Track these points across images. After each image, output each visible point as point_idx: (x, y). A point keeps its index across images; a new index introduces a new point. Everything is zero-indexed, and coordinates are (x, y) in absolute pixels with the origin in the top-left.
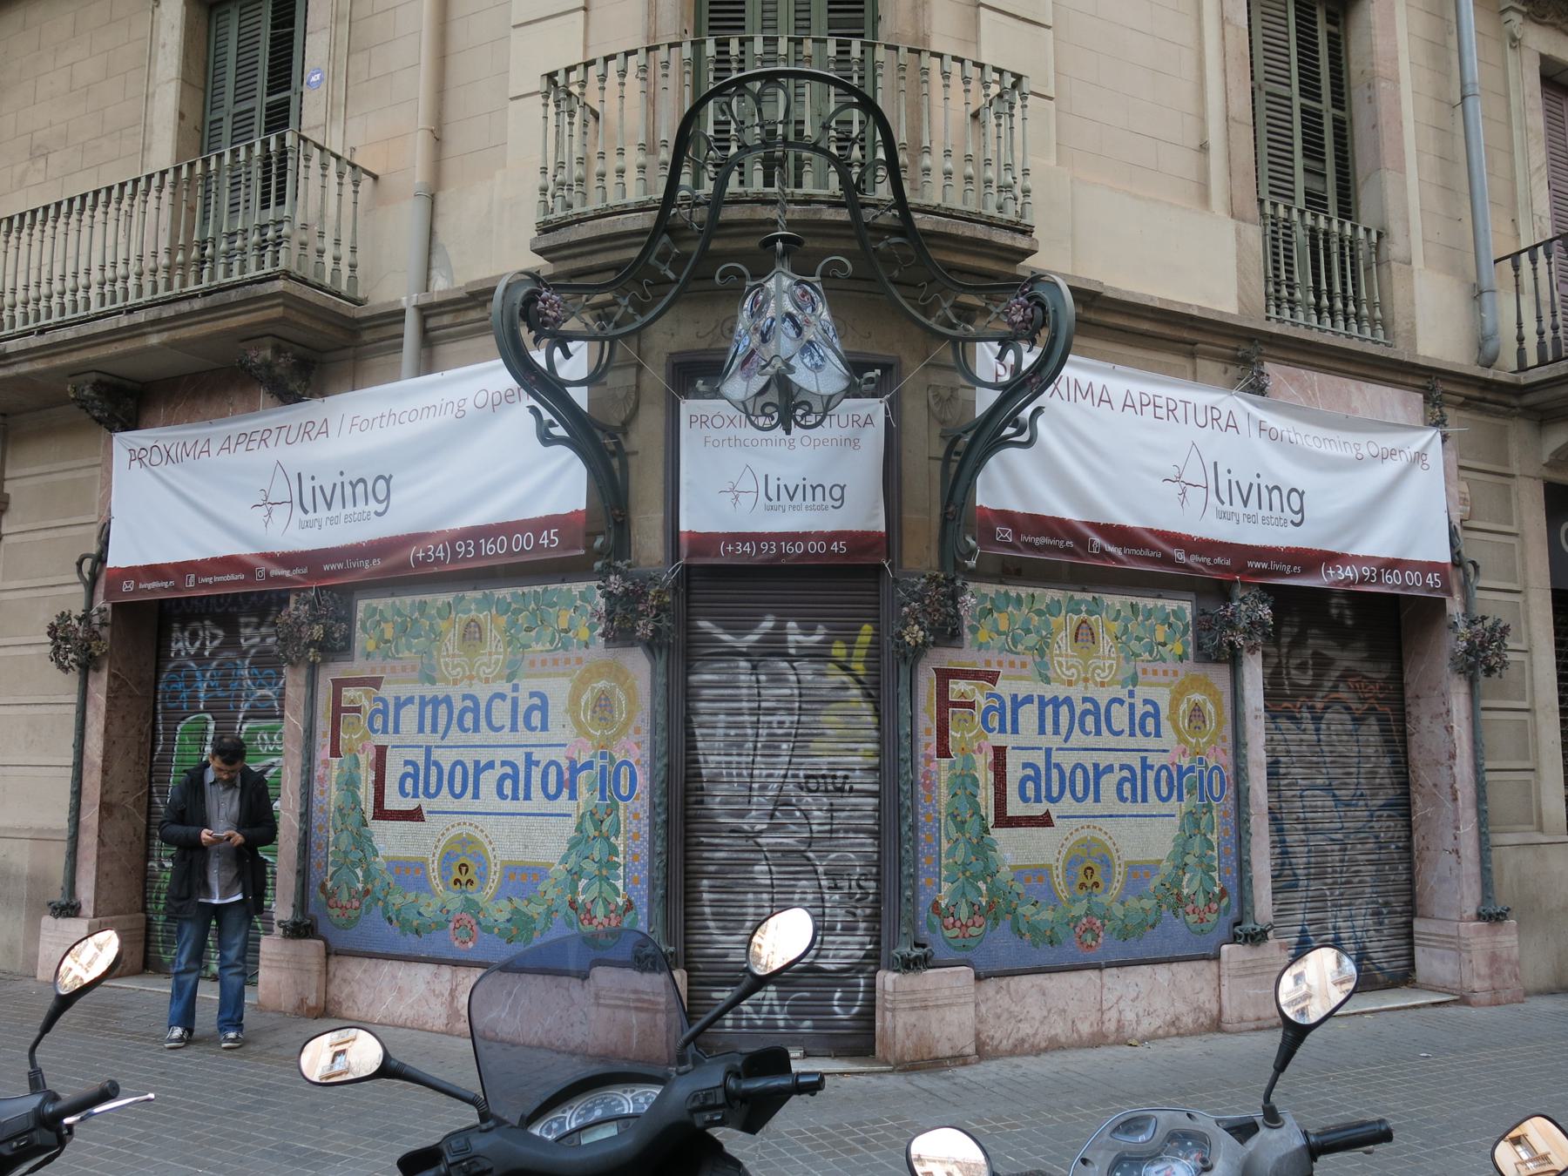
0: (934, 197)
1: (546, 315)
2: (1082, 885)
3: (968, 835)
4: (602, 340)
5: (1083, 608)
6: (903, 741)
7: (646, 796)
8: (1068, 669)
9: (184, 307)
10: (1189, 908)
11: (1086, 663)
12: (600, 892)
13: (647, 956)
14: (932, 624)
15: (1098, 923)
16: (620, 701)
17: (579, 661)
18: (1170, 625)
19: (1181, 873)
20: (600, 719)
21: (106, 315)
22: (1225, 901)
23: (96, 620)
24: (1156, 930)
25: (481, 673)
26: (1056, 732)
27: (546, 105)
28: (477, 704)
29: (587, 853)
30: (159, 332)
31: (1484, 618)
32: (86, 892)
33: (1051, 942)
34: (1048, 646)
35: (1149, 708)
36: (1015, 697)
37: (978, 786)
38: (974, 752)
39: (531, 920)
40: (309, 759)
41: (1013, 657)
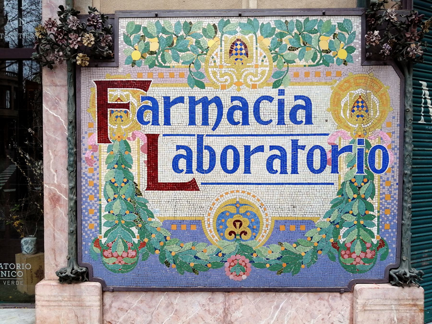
12: (359, 235)
20: (358, 116)
25: (248, 80)
29: (347, 209)
39: (301, 257)
40: (76, 145)
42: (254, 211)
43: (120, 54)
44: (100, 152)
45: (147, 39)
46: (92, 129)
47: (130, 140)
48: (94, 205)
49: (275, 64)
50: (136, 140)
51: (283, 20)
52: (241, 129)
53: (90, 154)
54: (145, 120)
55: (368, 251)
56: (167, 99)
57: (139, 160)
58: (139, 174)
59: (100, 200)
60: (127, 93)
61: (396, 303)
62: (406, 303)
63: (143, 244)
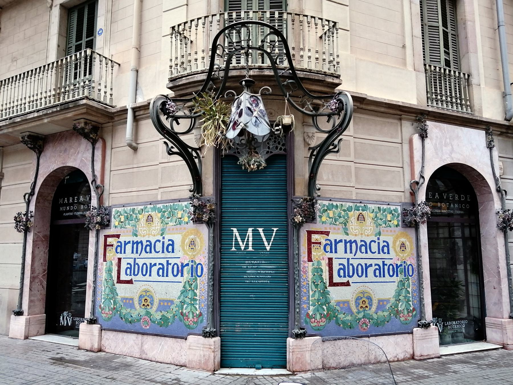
0: (305, 66)
1: (170, 110)
2: (361, 307)
3: (319, 289)
4: (191, 118)
5: (361, 209)
6: (295, 256)
7: (206, 275)
8: (355, 230)
9: (55, 110)
10: (401, 315)
11: (362, 228)
12: (191, 309)
13: (207, 332)
14: (305, 215)
15: (368, 321)
16: (198, 243)
17: (185, 229)
18: (393, 214)
19: (398, 302)
21: (31, 113)
22: (414, 313)
23: (29, 215)
24: (389, 323)
26: (351, 252)
27: (172, 38)
28: (151, 244)
30: (47, 118)
31: (509, 210)
32: (25, 307)
33: (350, 328)
34: (347, 222)
35: (385, 244)
36: (336, 240)
37: (322, 272)
38: (321, 260)
39: (168, 319)
40: (96, 263)
41: (334, 226)
42: (152, 294)
49: (162, 225)
51: (165, 205)
52: (149, 255)
55: (195, 318)
56: (125, 242)
61: (202, 346)
62: (207, 347)
63: (114, 308)
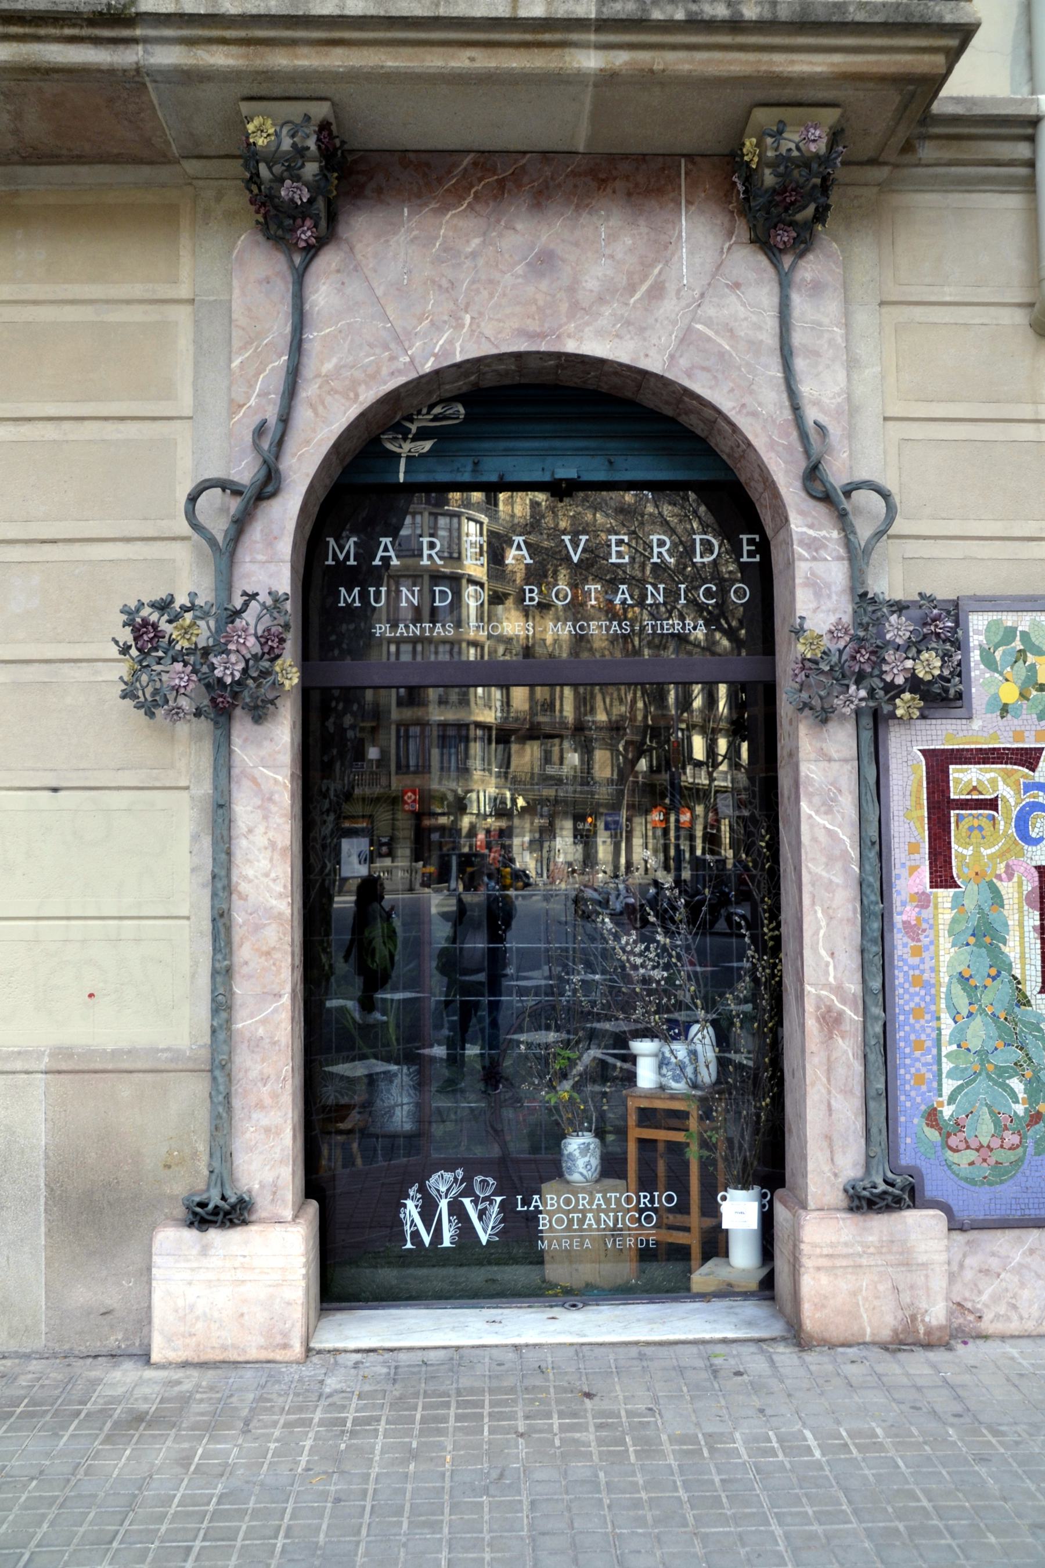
43: (973, 690)
44: (936, 907)
45: (1031, 659)
46: (917, 856)
47: (1001, 880)
48: (924, 1030)
50: (1015, 879)
53: (914, 914)
54: (1034, 835)
57: (1021, 925)
58: (1023, 957)
59: (938, 1019)
60: (993, 775)
